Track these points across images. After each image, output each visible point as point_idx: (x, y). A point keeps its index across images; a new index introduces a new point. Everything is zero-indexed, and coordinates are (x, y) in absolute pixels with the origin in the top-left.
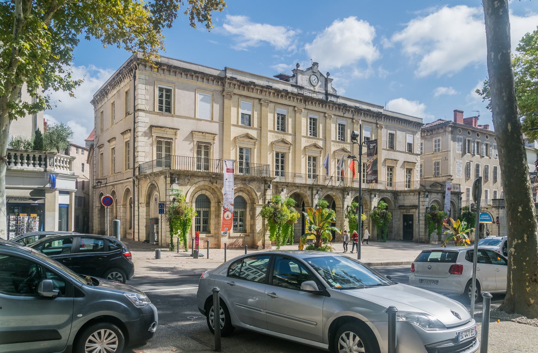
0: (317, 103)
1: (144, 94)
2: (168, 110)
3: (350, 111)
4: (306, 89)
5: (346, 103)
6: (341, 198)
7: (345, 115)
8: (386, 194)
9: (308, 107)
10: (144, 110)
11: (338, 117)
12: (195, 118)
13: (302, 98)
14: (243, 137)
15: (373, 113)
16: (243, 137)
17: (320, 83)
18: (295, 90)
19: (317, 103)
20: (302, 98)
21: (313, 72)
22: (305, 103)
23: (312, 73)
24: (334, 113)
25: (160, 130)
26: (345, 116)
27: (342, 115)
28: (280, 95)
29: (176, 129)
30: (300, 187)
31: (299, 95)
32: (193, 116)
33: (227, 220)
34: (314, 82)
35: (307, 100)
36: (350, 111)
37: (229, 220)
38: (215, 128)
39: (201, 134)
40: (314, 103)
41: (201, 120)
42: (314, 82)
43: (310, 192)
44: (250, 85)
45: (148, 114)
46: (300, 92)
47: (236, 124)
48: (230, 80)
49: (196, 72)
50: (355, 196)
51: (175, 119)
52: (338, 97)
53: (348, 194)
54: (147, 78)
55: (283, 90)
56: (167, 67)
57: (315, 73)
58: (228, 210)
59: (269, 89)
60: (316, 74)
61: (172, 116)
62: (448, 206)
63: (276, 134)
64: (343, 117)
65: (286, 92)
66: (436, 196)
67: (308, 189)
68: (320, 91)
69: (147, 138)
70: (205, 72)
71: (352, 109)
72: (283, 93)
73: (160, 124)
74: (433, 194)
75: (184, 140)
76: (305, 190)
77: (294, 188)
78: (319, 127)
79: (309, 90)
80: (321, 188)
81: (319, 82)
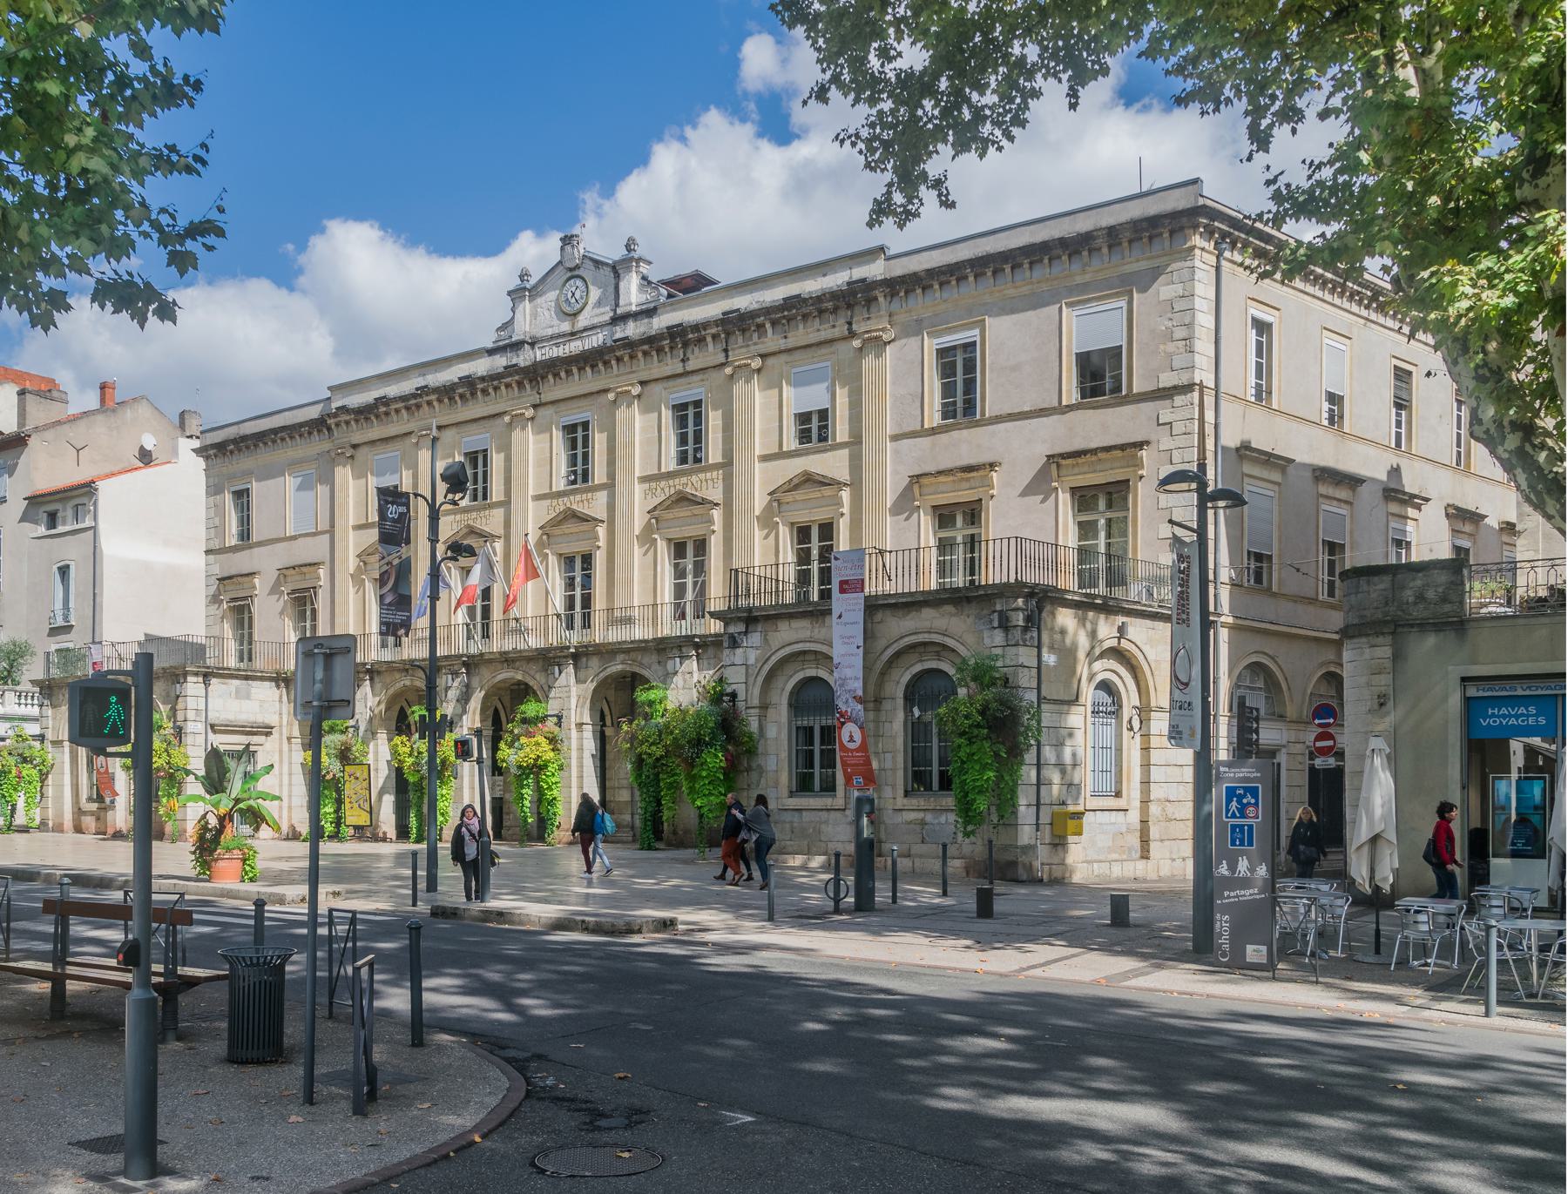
0: (575, 370)
7: (691, 366)
9: (546, 397)
11: (671, 383)
13: (517, 378)
15: (819, 299)
18: (500, 362)
19: (575, 370)
20: (517, 378)
21: (571, 270)
24: (645, 376)
27: (680, 370)
28: (457, 398)
31: (511, 370)
33: (852, 751)
35: (535, 375)
37: (857, 750)
46: (514, 361)
47: (364, 522)
49: (275, 431)
50: (602, 675)
55: (460, 379)
57: (577, 267)
58: (850, 719)
59: (420, 396)
62: (848, 672)
65: (469, 382)
66: (807, 634)
70: (288, 423)
71: (714, 331)
72: (461, 391)
74: (783, 625)
77: (397, 676)
79: (552, 338)
80: (465, 664)
81: (591, 287)
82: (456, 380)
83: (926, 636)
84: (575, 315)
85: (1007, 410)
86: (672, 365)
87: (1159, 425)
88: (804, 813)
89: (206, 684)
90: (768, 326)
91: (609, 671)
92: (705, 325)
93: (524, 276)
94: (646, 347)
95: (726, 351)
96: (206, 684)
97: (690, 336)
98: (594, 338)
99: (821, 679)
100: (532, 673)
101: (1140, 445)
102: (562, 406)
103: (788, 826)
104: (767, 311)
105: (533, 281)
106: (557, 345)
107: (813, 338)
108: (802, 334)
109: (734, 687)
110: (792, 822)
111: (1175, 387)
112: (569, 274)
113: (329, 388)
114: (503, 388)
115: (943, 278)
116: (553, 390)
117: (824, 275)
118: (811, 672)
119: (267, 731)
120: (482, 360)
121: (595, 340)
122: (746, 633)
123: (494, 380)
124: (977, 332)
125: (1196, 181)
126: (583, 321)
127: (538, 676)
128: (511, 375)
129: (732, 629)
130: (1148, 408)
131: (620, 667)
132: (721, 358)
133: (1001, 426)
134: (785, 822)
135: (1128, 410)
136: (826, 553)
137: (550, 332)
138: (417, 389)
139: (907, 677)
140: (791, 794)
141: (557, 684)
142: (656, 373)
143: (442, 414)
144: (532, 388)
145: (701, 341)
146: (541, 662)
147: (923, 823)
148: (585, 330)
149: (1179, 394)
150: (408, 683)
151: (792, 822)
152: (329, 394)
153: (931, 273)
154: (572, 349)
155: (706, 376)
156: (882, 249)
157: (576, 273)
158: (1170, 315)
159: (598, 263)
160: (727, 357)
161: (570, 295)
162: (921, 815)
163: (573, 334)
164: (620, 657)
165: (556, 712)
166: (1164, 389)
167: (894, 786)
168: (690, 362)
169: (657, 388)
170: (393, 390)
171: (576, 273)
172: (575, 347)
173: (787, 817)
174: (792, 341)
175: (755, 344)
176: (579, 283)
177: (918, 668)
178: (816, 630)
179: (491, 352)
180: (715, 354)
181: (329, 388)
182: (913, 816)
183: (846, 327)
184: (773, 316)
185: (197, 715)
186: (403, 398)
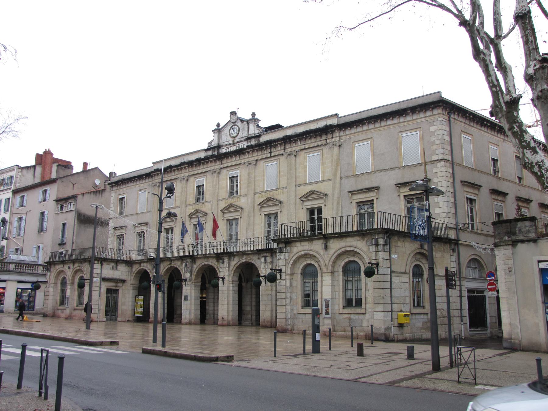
7: (273, 154)
9: (225, 165)
13: (214, 159)
18: (210, 153)
20: (214, 159)
26: (272, 155)
27: (269, 155)
59: (182, 165)
64: (271, 157)
79: (226, 145)
82: (194, 160)
83: (349, 248)
84: (234, 137)
88: (307, 315)
89: (102, 264)
93: (218, 125)
96: (102, 264)
98: (241, 145)
99: (313, 265)
102: (229, 169)
103: (301, 320)
105: (221, 127)
107: (314, 145)
109: (281, 267)
110: (302, 318)
112: (233, 125)
113: (152, 163)
118: (309, 262)
119: (123, 281)
121: (240, 146)
122: (285, 247)
129: (281, 246)
131: (245, 260)
134: (299, 318)
136: (320, 219)
137: (226, 143)
139: (343, 263)
140: (302, 308)
142: (261, 157)
145: (275, 146)
147: (350, 319)
151: (302, 318)
152: (152, 165)
154: (233, 149)
155: (278, 158)
162: (348, 316)
163: (233, 144)
164: (245, 257)
165: (222, 277)
167: (339, 305)
168: (273, 153)
172: (234, 148)
173: (301, 316)
174: (307, 146)
175: (294, 147)
177: (347, 260)
181: (152, 163)
182: (346, 316)
185: (97, 276)
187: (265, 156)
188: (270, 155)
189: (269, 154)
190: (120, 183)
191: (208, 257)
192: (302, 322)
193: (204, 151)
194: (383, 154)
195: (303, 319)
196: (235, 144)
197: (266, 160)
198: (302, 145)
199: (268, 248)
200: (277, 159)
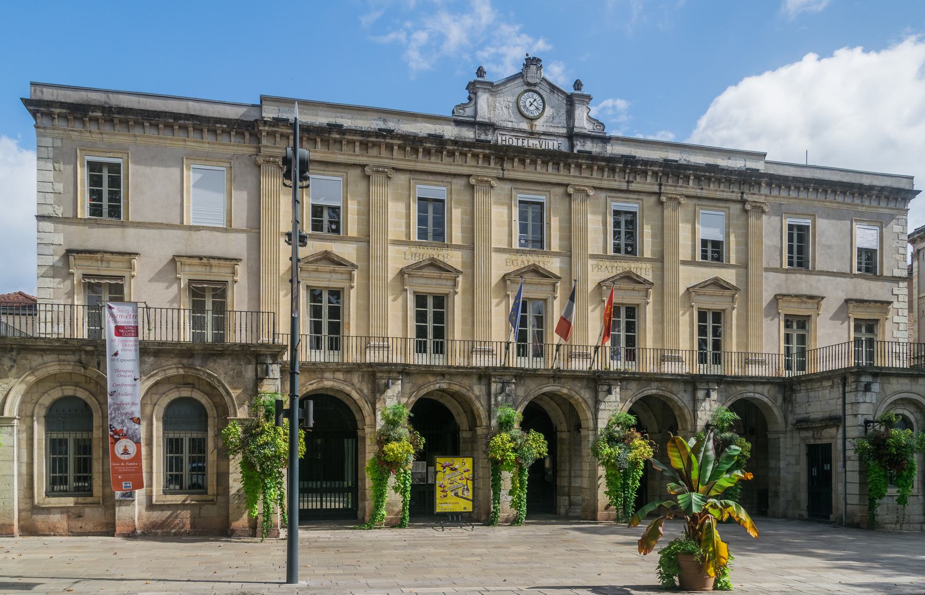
0: (539, 162)
1: (52, 180)
2: (115, 212)
3: (650, 173)
4: (504, 129)
5: (633, 154)
6: (590, 402)
7: (633, 187)
8: (751, 388)
9: (507, 174)
10: (50, 217)
12: (181, 226)
13: (487, 151)
14: (316, 261)
15: (730, 172)
16: (316, 261)
17: (549, 111)
18: (468, 134)
20: (487, 151)
21: (528, 84)
22: (502, 165)
23: (526, 88)
24: (596, 183)
25: (91, 258)
27: (624, 186)
28: (421, 150)
29: (130, 254)
30: (451, 374)
32: (177, 222)
34: (533, 108)
35: (503, 154)
36: (650, 173)
38: (237, 245)
39: (196, 261)
40: (528, 161)
41: (197, 229)
42: (533, 108)
43: (484, 388)
44: (330, 133)
45: (60, 226)
46: (483, 137)
48: (270, 126)
49: (177, 116)
50: (640, 396)
51: (131, 231)
52: (605, 140)
53: (609, 392)
54: (58, 143)
55: (429, 135)
56: (103, 112)
57: (535, 85)
59: (384, 137)
60: (537, 89)
61: (123, 225)
63: (414, 250)
65: (439, 140)
66: (907, 388)
67: (475, 380)
68: (552, 130)
69: (58, 280)
70: (204, 114)
71: (656, 169)
72: (428, 145)
73: (90, 246)
74: (894, 380)
75: (150, 281)
76: (466, 382)
77: (432, 379)
78: (549, 224)
79: (513, 130)
80: (515, 377)
85: (825, 269)
86: (618, 182)
87: (893, 294)
90: (692, 177)
91: (645, 393)
92: (652, 163)
94: (604, 164)
95: (660, 185)
97: (639, 167)
98: (551, 143)
100: (577, 389)
101: (890, 303)
102: (520, 186)
103: (885, 506)
104: (696, 168)
106: (517, 138)
107: (719, 195)
108: (712, 190)
111: (900, 277)
112: (526, 88)
114: (469, 155)
115: (798, 184)
116: (515, 171)
117: (729, 159)
120: (449, 127)
123: (460, 147)
124: (810, 221)
125: (912, 178)
126: (540, 126)
127: (582, 392)
128: (483, 148)
130: (888, 285)
131: (654, 391)
132: (656, 189)
133: (823, 277)
135: (879, 283)
137: (510, 125)
138: (380, 130)
141: (606, 399)
142: (605, 184)
143: (398, 159)
144: (496, 164)
145: (644, 173)
146: (585, 382)
148: (545, 134)
149: (902, 281)
150: (444, 386)
153: (795, 179)
154: (530, 144)
155: (640, 197)
156: (765, 155)
157: (532, 88)
158: (897, 240)
159: (553, 88)
160: (660, 189)
161: (528, 104)
163: (532, 134)
164: (654, 385)
166: (895, 277)
168: (633, 185)
169: (603, 195)
170: (347, 122)
171: (532, 88)
172: (533, 143)
174: (705, 193)
176: (536, 96)
178: (914, 386)
179: (459, 123)
180: (653, 184)
183: (740, 195)
184: (698, 173)
186: (363, 133)
187: (615, 185)
188: (628, 186)
189: (626, 184)
190: (99, 114)
191: (560, 378)
192: (888, 510)
193: (453, 124)
194: (830, 247)
195: (890, 505)
196: (537, 136)
197: (613, 194)
198: (696, 189)
199: (733, 374)
200: (638, 199)
